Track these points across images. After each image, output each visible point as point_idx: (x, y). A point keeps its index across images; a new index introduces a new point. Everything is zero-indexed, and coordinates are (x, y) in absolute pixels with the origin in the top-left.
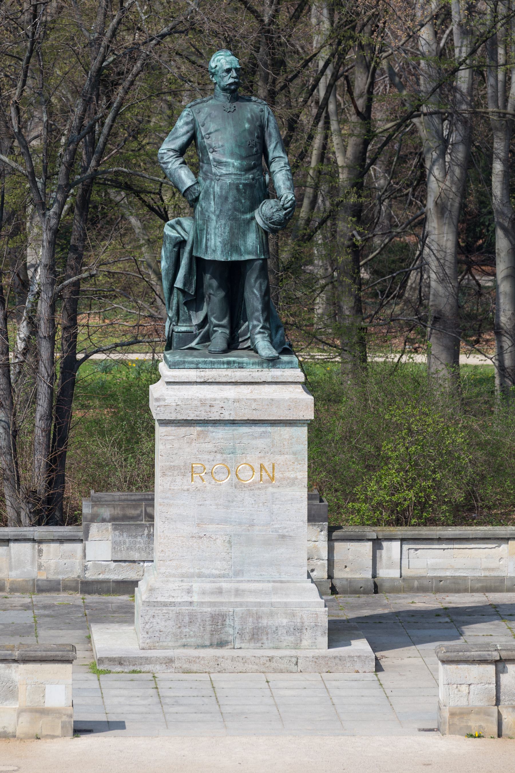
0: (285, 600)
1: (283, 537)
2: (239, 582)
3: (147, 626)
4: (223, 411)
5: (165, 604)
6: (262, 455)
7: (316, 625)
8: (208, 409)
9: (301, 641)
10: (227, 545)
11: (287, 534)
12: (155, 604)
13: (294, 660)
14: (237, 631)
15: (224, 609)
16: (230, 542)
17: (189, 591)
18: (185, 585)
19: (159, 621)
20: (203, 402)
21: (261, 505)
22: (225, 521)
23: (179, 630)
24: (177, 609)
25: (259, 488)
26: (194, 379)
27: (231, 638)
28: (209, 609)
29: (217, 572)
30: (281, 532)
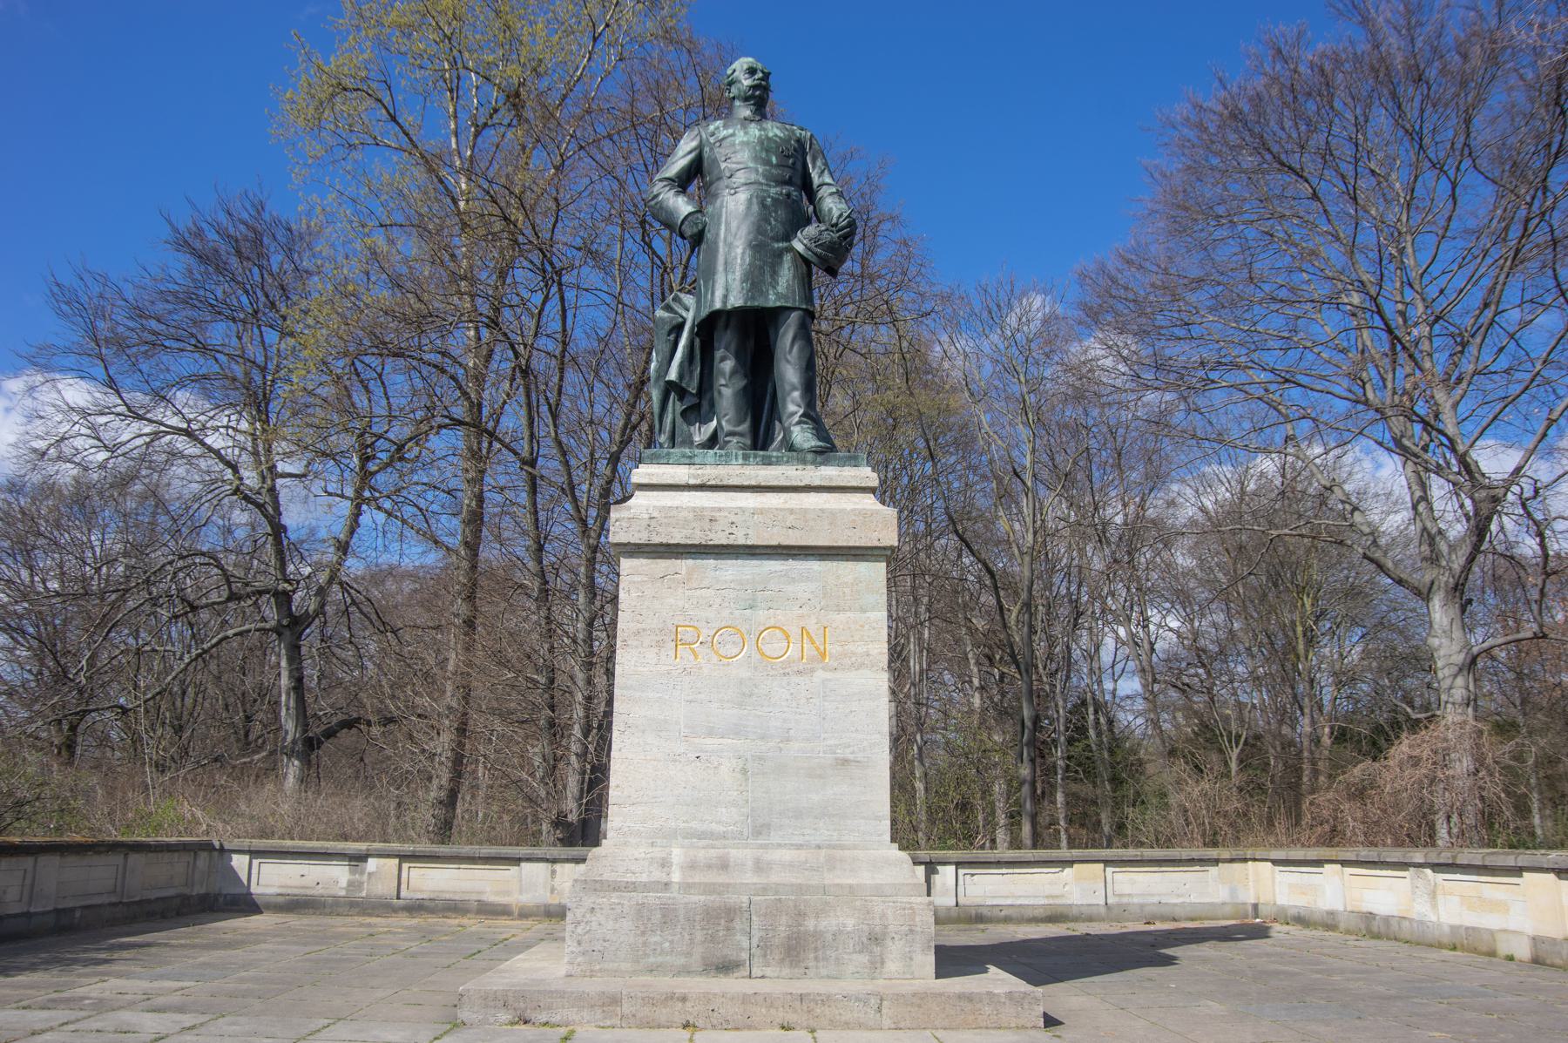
0: (850, 881)
1: (845, 762)
2: (762, 847)
3: (579, 930)
4: (734, 530)
5: (616, 887)
6: (804, 610)
7: (911, 931)
8: (707, 526)
9: (883, 963)
10: (739, 776)
11: (851, 757)
12: (598, 886)
13: (873, 1001)
14: (755, 941)
15: (733, 899)
16: (744, 771)
17: (665, 864)
18: (658, 853)
19: (602, 919)
20: (698, 514)
21: (803, 701)
22: (737, 731)
23: (641, 939)
24: (638, 897)
25: (799, 672)
26: (683, 480)
27: (744, 956)
28: (702, 898)
29: (722, 829)
30: (840, 753)
